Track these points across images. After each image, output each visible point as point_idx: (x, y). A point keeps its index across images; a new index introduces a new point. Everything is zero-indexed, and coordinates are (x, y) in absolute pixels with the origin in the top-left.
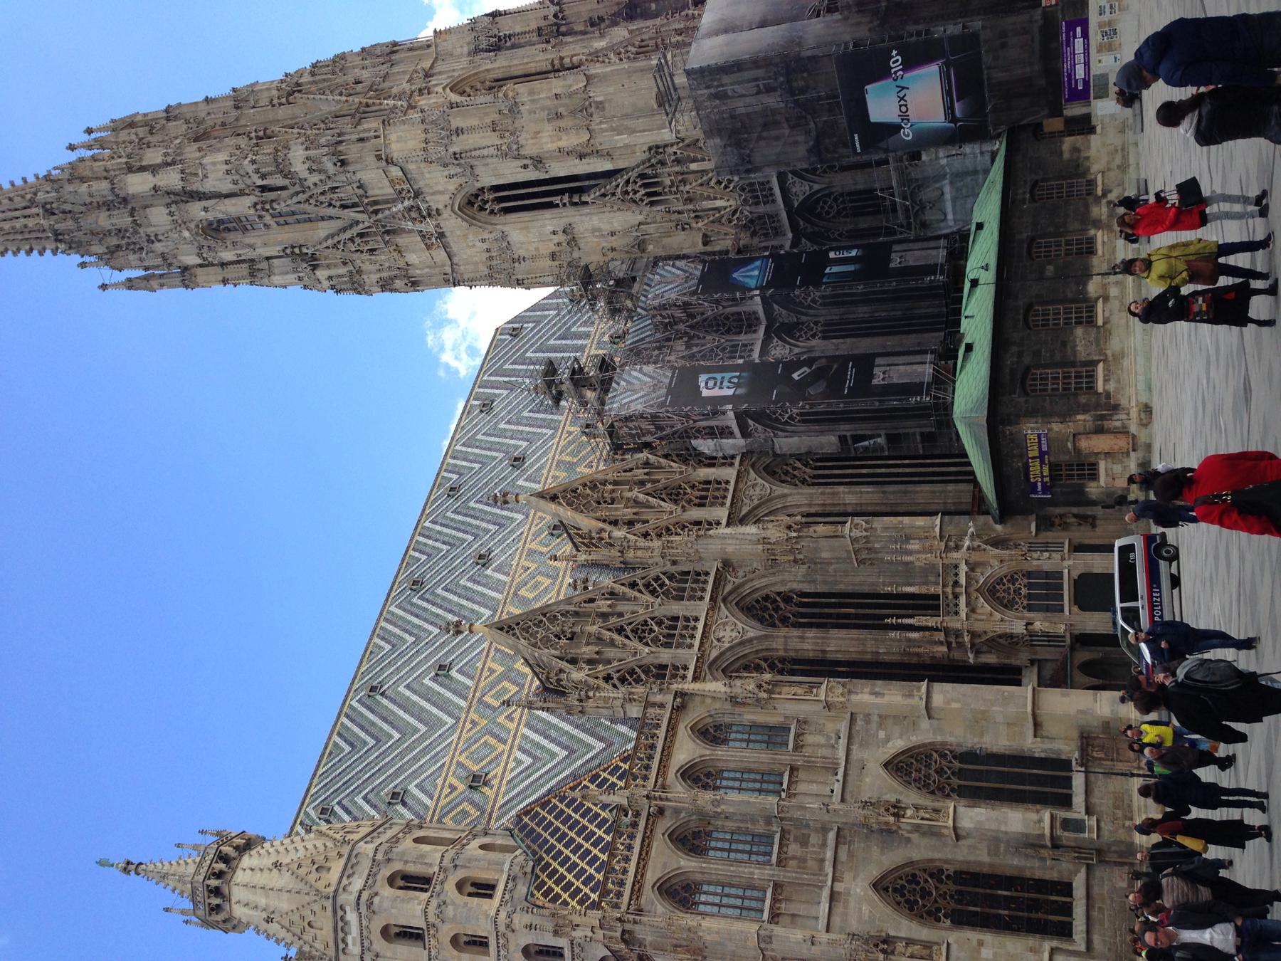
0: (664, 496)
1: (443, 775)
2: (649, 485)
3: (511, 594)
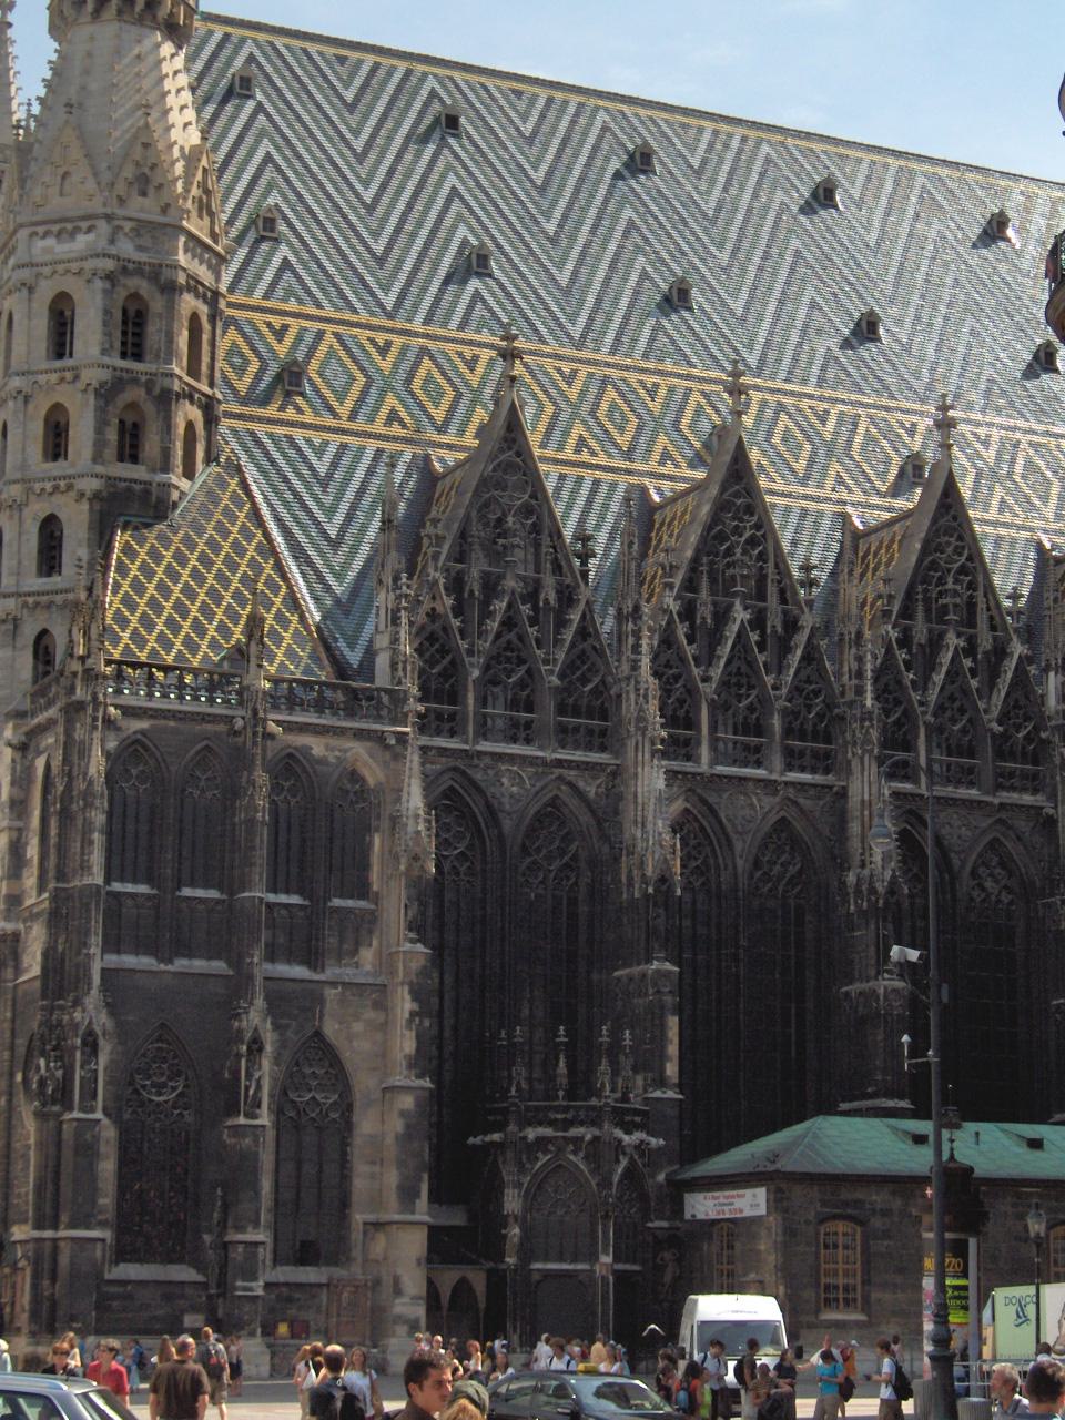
0: (736, 664)
1: (303, 309)
2: (754, 637)
3: (608, 371)
